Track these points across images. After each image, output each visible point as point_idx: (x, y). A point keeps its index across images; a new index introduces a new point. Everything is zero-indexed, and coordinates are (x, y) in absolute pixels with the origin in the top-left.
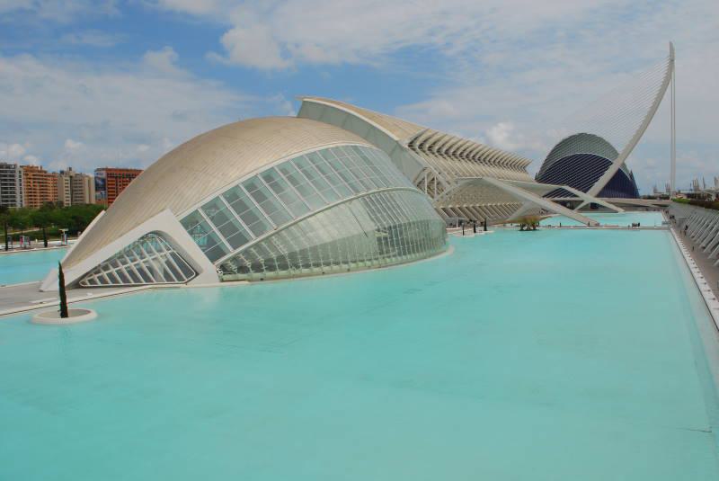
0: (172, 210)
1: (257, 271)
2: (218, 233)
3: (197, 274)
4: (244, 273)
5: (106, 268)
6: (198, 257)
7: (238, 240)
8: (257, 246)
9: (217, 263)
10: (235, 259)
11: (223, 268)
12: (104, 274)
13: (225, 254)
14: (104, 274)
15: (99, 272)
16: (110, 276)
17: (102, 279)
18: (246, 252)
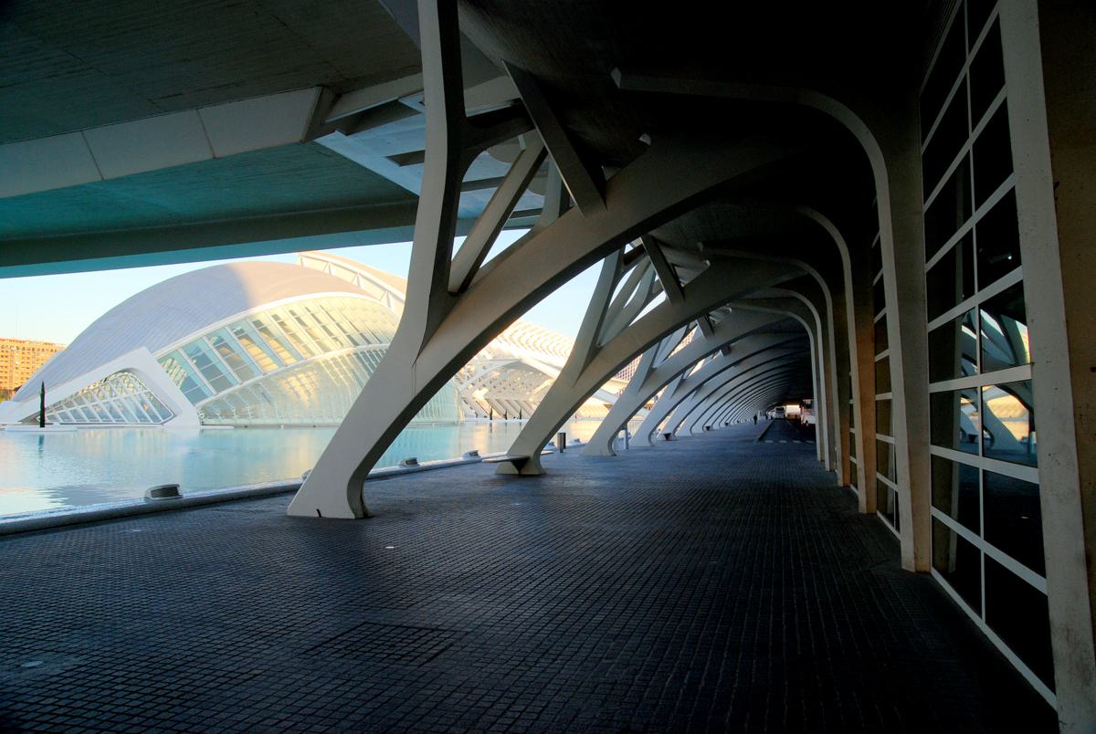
0: (149, 349)
1: (241, 417)
2: (201, 375)
3: (175, 416)
4: (227, 417)
5: (69, 404)
6: (178, 399)
7: (221, 383)
8: (243, 391)
9: (197, 405)
10: (217, 402)
11: (208, 413)
12: (67, 411)
13: (206, 397)
14: (67, 411)
15: (61, 408)
16: (74, 412)
17: (64, 416)
18: (231, 396)
